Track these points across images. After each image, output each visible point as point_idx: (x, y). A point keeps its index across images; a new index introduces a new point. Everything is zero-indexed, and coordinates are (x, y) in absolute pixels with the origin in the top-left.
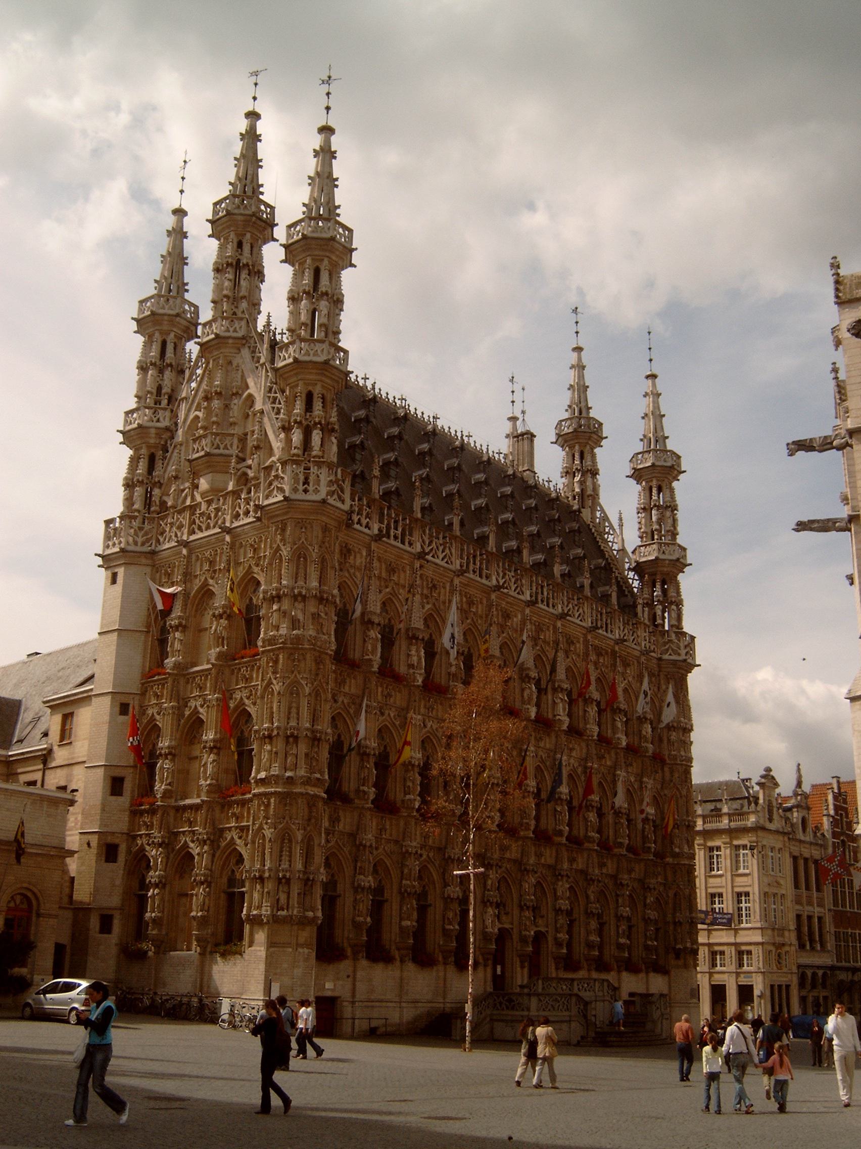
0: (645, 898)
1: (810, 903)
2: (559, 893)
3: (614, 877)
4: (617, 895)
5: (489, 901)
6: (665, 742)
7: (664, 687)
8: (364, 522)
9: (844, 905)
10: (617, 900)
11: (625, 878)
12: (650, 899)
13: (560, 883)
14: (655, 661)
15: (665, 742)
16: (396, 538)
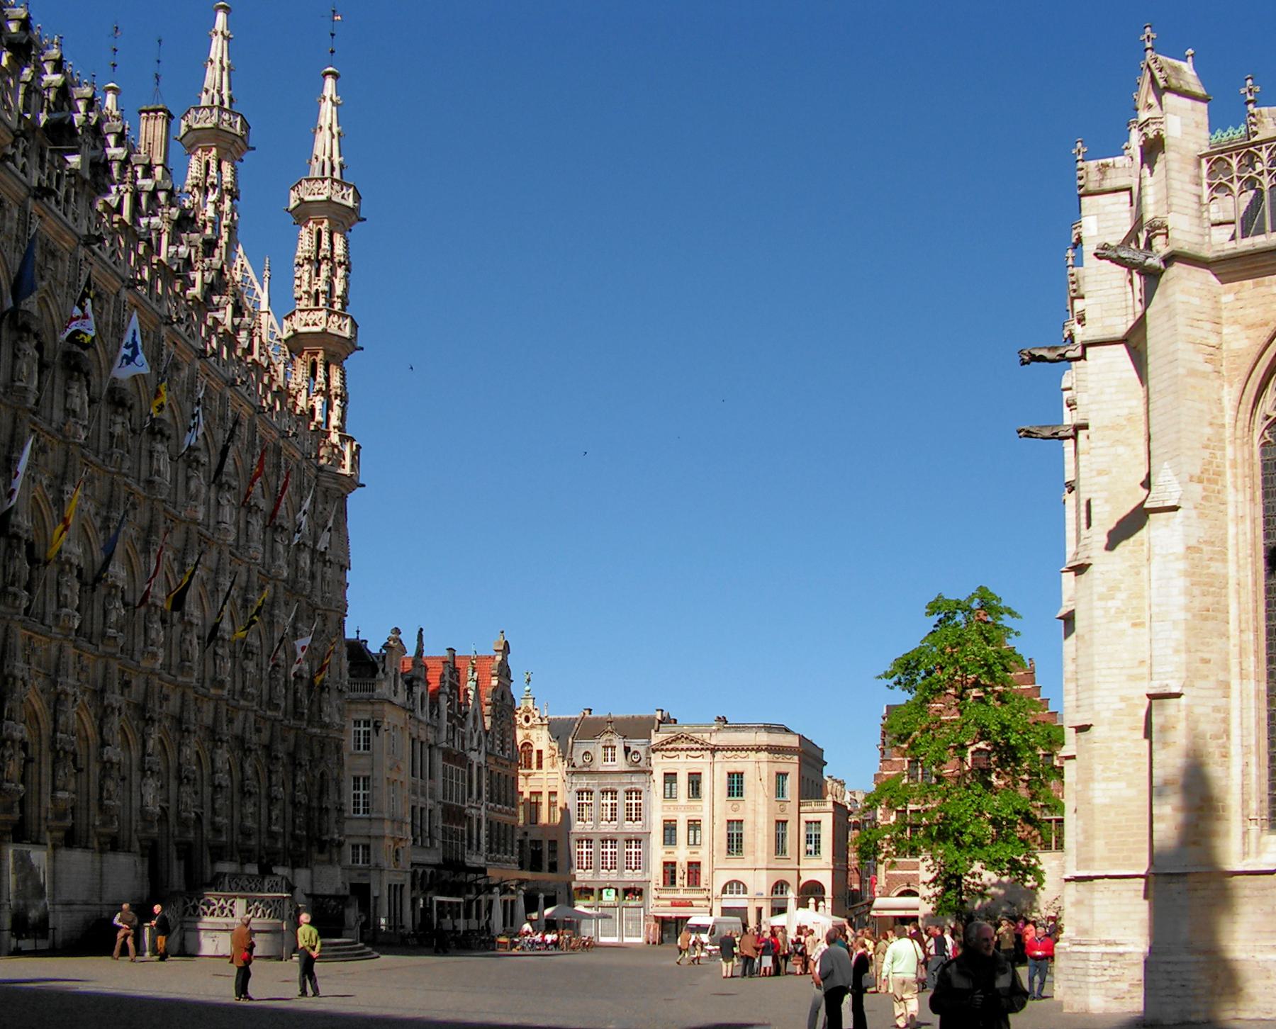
0: (295, 776)
1: (423, 794)
2: (219, 764)
3: (268, 748)
4: (270, 772)
5: (150, 769)
6: (319, 578)
7: (320, 507)
8: (21, 161)
9: (451, 799)
10: (270, 779)
11: (281, 750)
12: (301, 779)
13: (220, 751)
14: (314, 471)
15: (319, 578)
16: (58, 203)
